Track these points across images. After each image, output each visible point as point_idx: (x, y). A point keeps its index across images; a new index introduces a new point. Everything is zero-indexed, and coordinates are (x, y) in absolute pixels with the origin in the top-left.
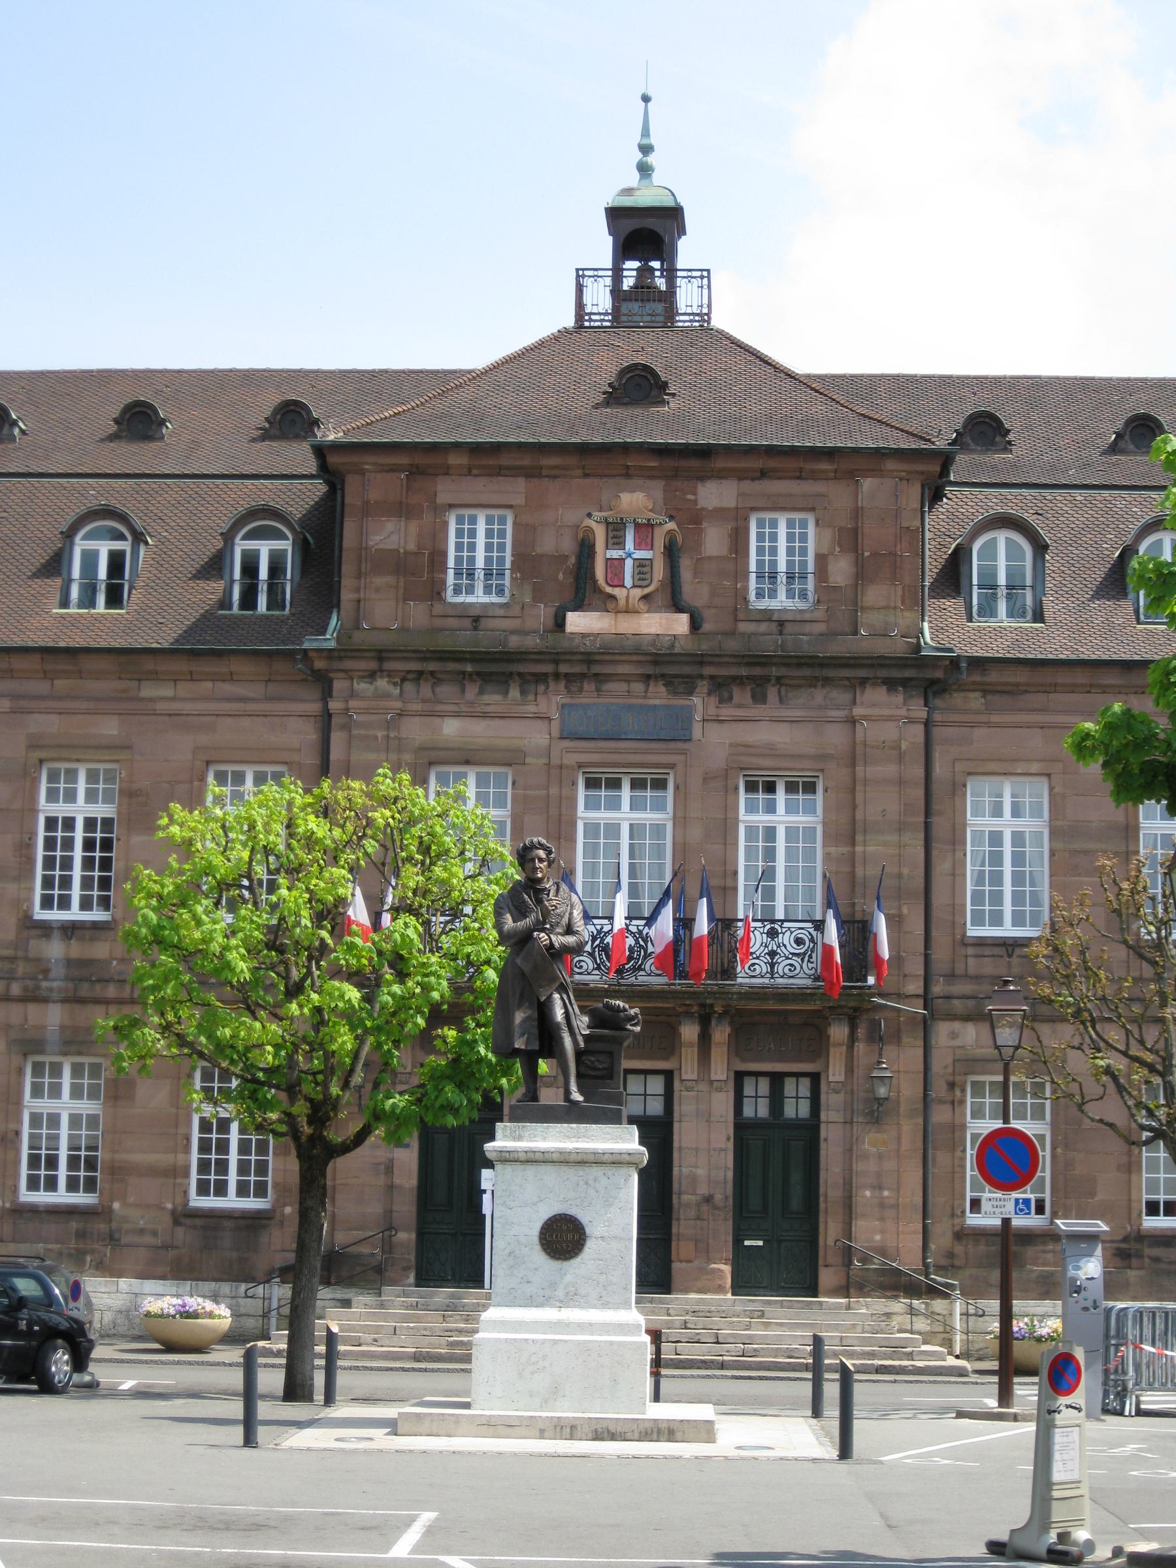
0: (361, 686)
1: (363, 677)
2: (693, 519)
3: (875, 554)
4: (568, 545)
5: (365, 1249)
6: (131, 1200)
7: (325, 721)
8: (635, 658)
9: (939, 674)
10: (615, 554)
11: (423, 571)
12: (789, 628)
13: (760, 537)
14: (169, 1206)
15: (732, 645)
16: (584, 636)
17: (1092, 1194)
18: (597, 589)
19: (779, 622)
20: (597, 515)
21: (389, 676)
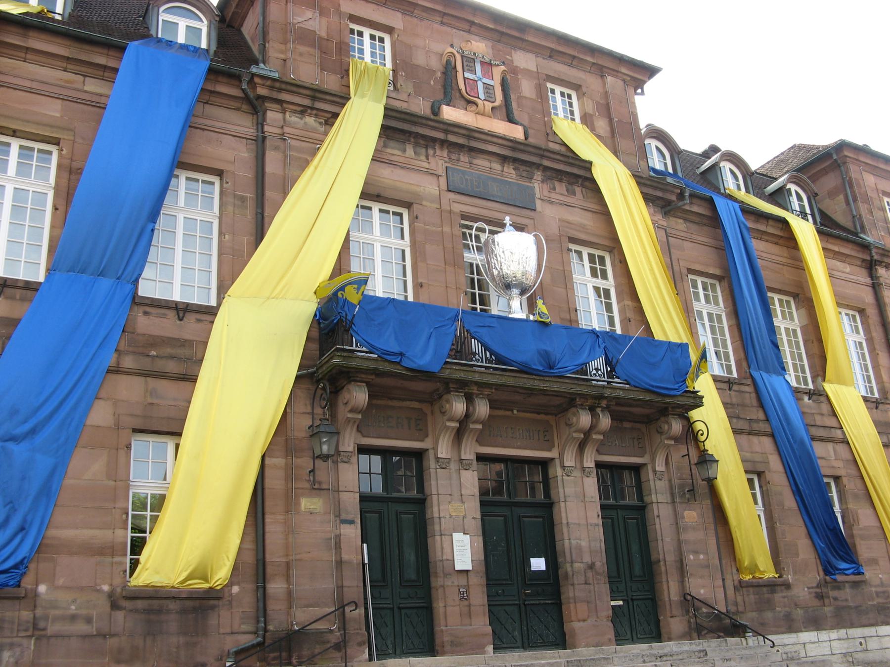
0: (293, 119)
1: (295, 112)
3: (619, 121)
5: (321, 626)
6: (61, 582)
7: (260, 142)
8: (500, 141)
9: (674, 198)
14: (106, 588)
21: (316, 116)
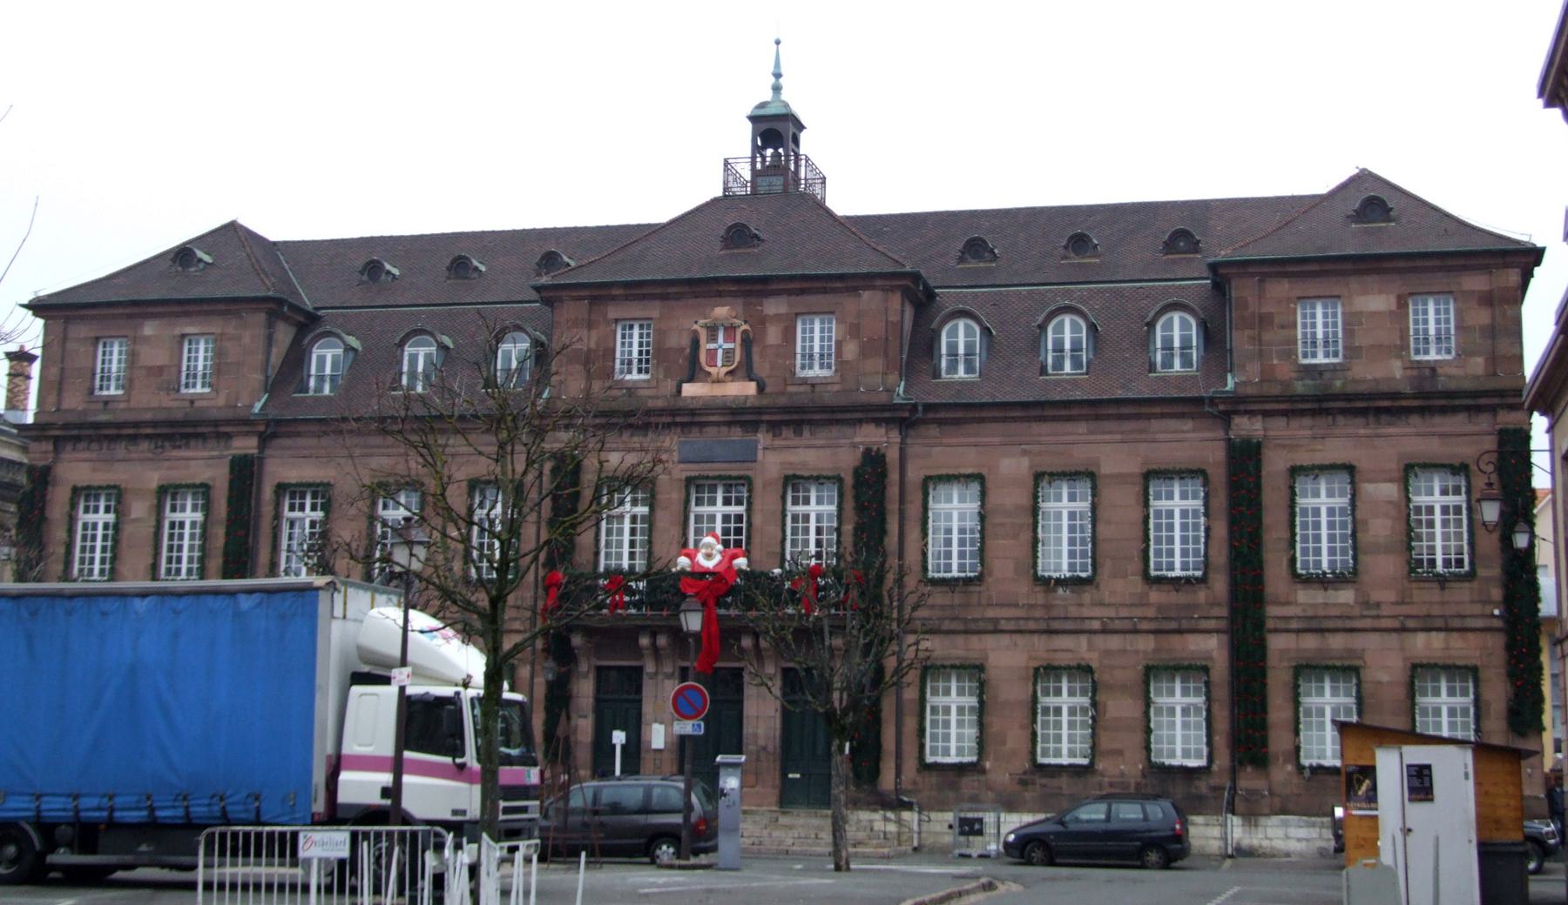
2: (761, 322)
4: (685, 341)
9: (906, 414)
10: (712, 346)
11: (599, 361)
12: (818, 389)
13: (804, 331)
15: (782, 401)
16: (693, 398)
17: (1004, 743)
18: (701, 369)
19: (813, 384)
20: (702, 322)
